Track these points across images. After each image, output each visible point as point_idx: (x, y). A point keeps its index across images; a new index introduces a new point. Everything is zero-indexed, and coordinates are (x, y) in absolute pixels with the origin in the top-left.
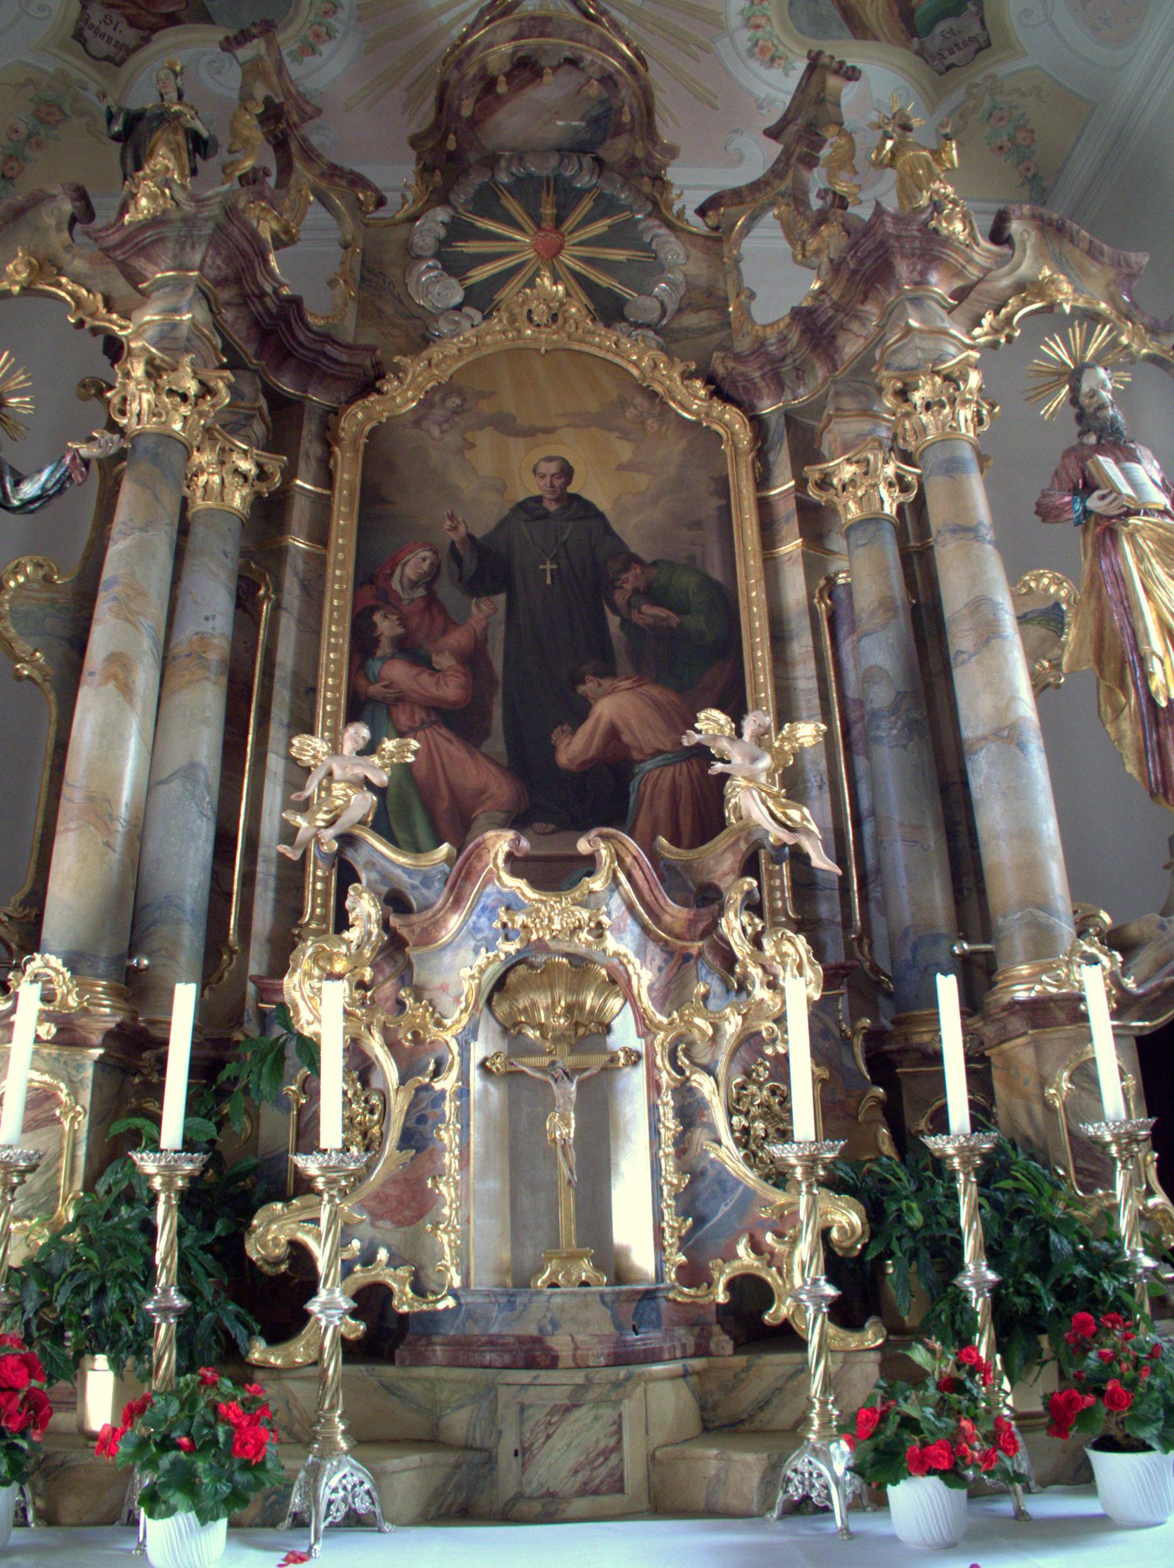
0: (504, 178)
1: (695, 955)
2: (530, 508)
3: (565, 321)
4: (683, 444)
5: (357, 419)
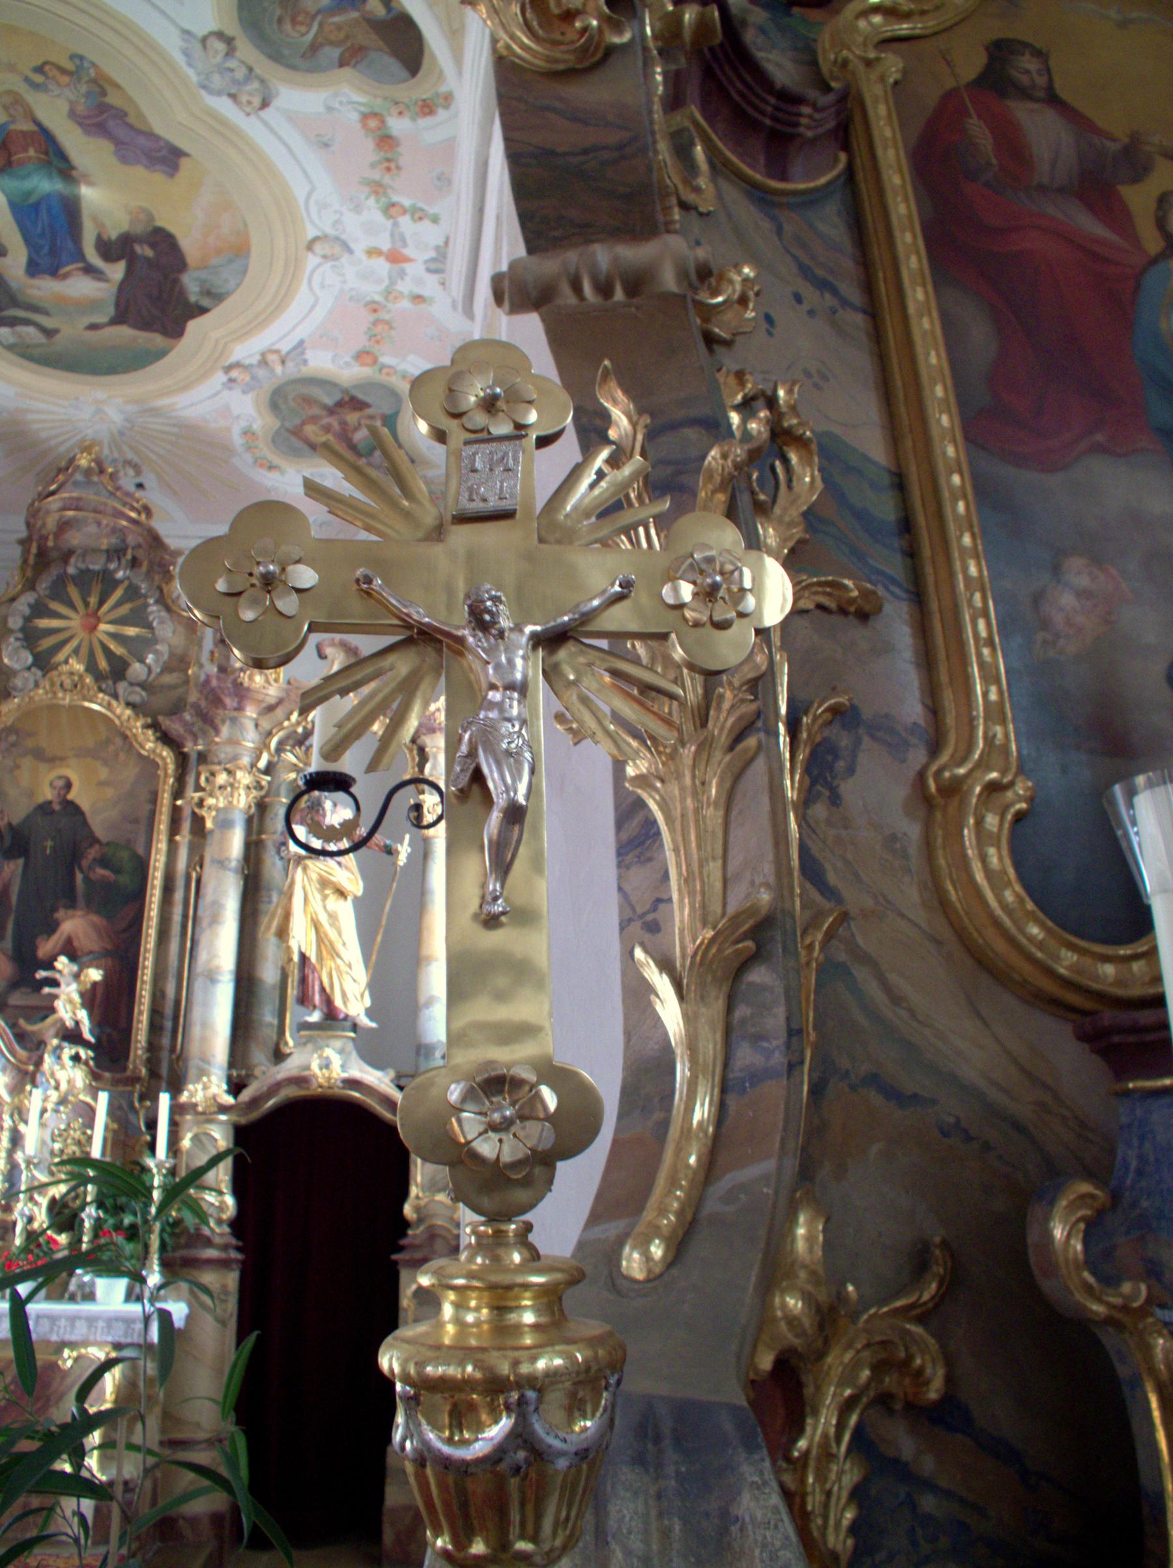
0: (71, 570)
2: (44, 809)
3: (83, 687)
4: (137, 770)
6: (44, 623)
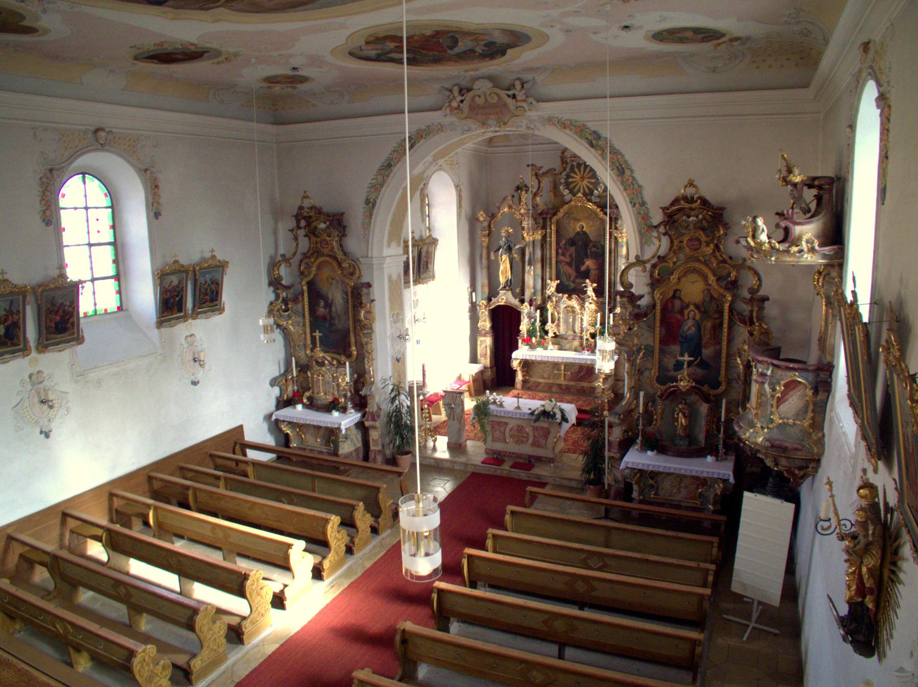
2: (578, 233)
5: (554, 219)
6: (570, 180)
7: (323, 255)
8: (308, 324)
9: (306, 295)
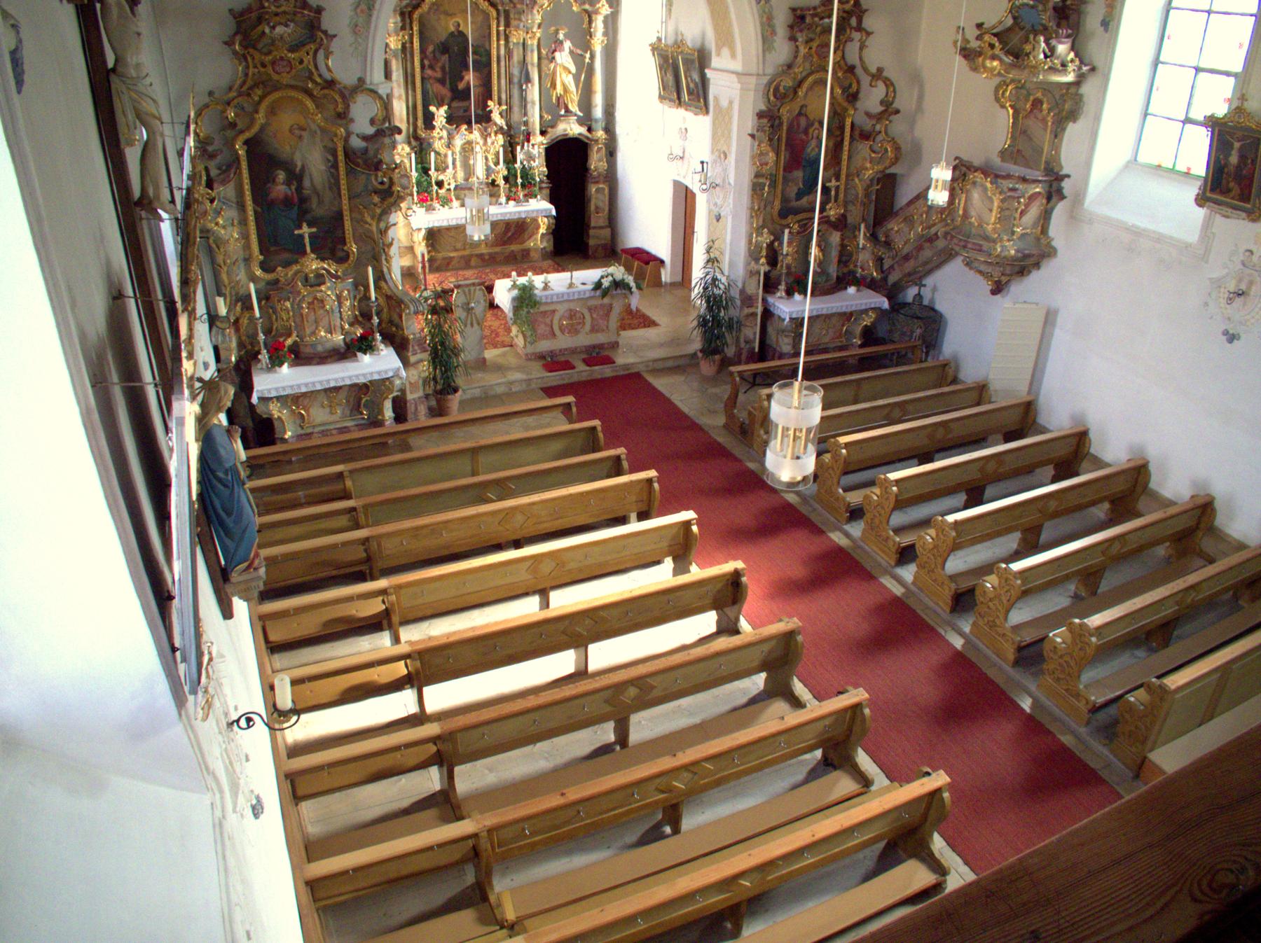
1: (485, 137)
5: (416, 16)
7: (276, 88)
8: (251, 218)
9: (244, 165)
